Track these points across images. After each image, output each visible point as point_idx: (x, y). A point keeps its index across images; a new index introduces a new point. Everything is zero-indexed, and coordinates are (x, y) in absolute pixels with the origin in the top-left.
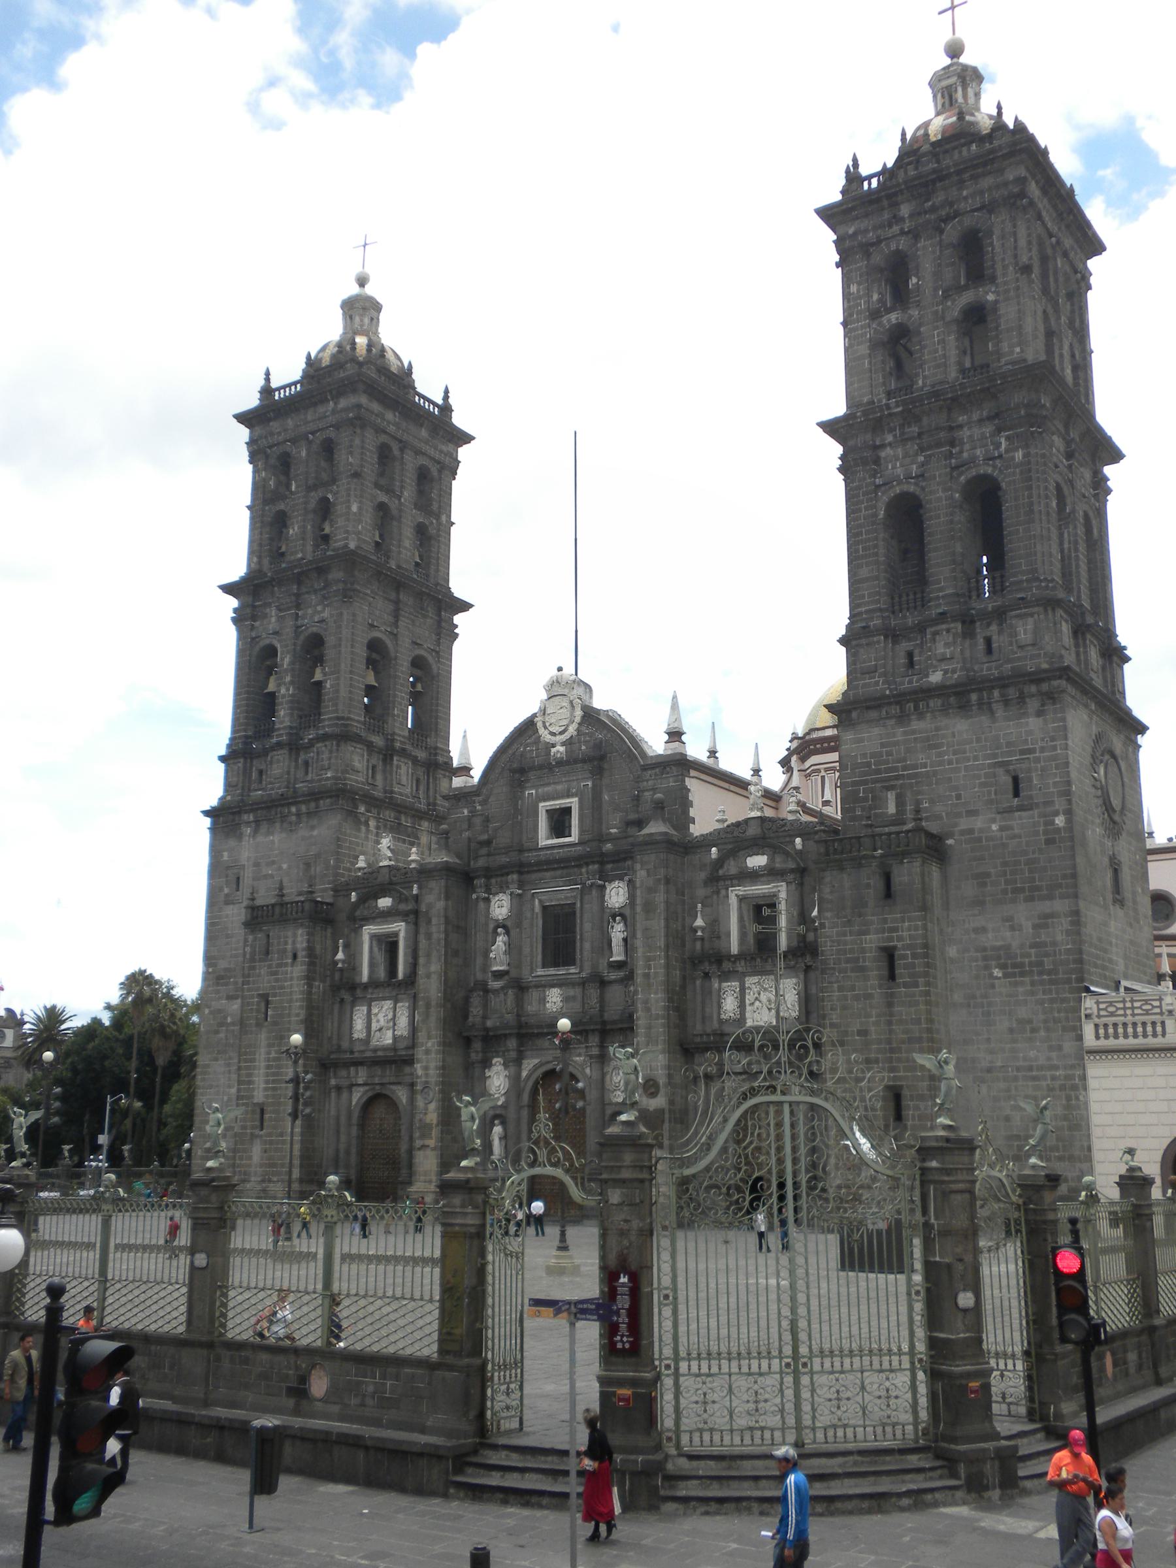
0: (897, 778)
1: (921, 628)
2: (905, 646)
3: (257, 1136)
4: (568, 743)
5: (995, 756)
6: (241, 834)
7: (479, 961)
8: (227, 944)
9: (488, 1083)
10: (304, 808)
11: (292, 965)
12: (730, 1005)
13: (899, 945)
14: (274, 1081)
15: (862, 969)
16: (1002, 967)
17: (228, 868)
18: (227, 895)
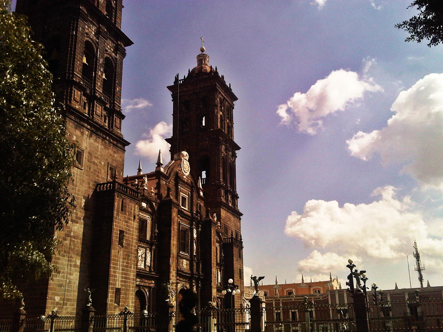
8: (73, 189)
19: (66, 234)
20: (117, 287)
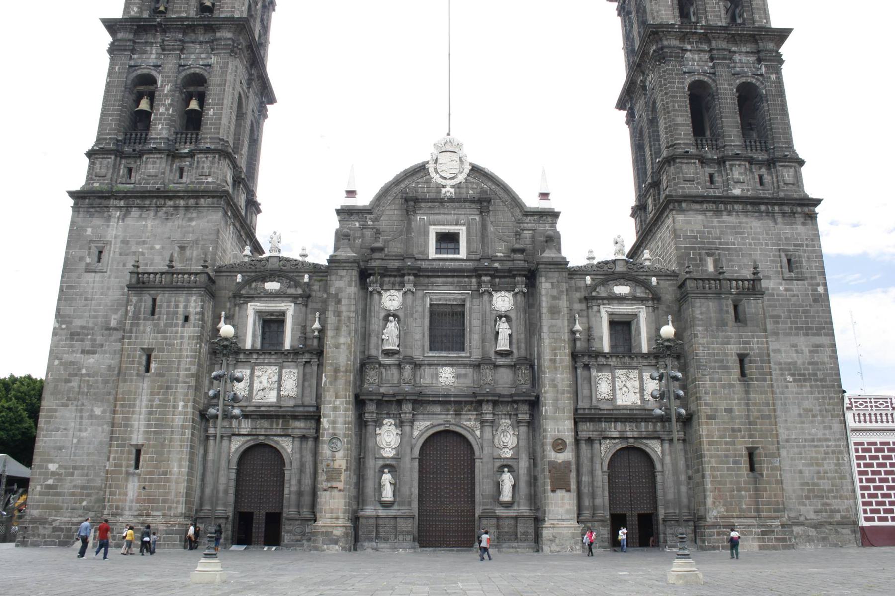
0: (717, 249)
1: (721, 162)
2: (708, 170)
3: (134, 474)
4: (458, 187)
5: (778, 245)
7: (374, 340)
9: (378, 438)
10: (182, 203)
11: (183, 326)
12: (604, 389)
13: (751, 353)
14: (156, 426)
15: (726, 367)
16: (792, 375)
17: (90, 242)
18: (88, 264)
19: (70, 375)
20: (134, 442)
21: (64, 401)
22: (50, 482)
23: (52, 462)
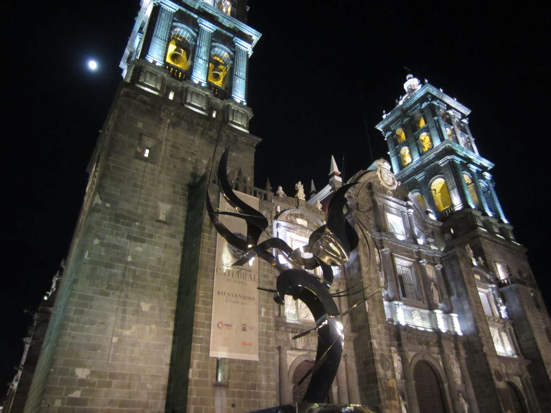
4: (393, 191)
6: (161, 120)
18: (137, 153)
21: (104, 288)
22: (77, 394)
23: (81, 365)
